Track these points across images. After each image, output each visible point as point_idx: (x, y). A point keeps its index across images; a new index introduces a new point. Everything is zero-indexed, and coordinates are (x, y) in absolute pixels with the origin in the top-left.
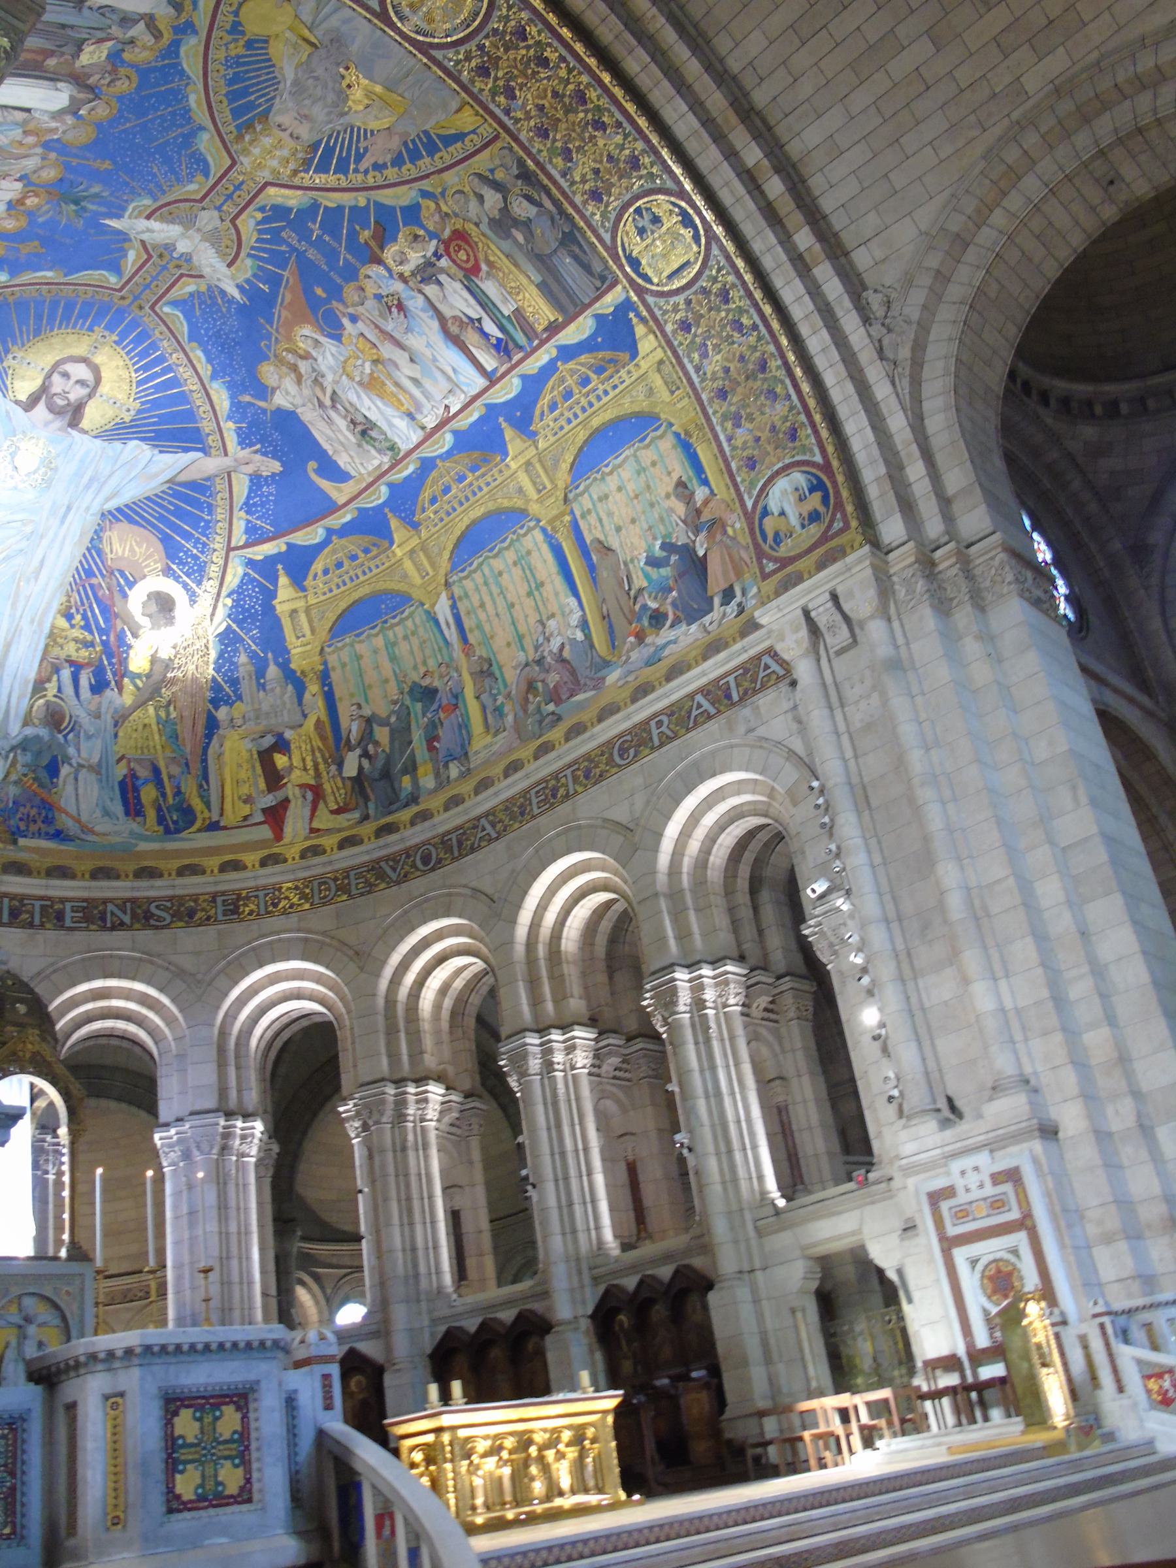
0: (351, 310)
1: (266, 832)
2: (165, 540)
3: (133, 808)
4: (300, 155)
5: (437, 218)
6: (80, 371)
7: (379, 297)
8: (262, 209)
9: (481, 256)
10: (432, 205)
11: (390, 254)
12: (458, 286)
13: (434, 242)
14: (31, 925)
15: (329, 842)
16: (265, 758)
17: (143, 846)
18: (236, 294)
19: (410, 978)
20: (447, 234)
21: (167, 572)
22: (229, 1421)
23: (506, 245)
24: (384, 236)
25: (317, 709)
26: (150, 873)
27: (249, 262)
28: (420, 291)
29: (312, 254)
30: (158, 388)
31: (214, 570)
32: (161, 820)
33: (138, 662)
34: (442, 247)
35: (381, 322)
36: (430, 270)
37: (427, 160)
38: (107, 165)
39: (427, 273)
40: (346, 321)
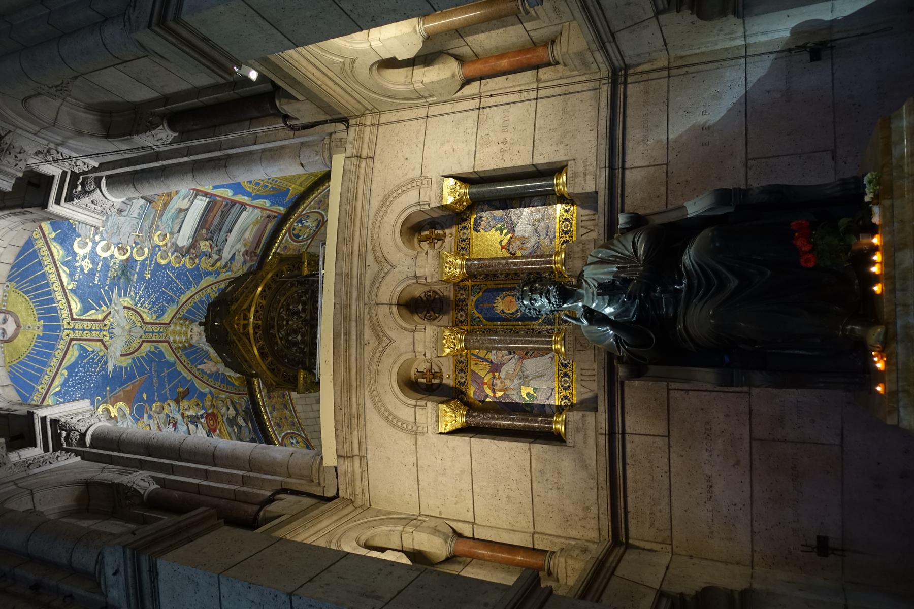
0: (151, 412)
4: (186, 344)
5: (210, 404)
7: (168, 415)
8: (156, 348)
9: (218, 427)
10: (211, 399)
11: (184, 404)
12: (204, 432)
13: (203, 411)
18: (110, 368)
20: (210, 411)
23: (230, 430)
24: (186, 395)
27: (130, 361)
28: (187, 425)
29: (155, 381)
30: (25, 374)
34: (205, 415)
35: (162, 426)
36: (196, 419)
37: (219, 383)
38: (148, 276)
39: (194, 420)
40: (146, 416)
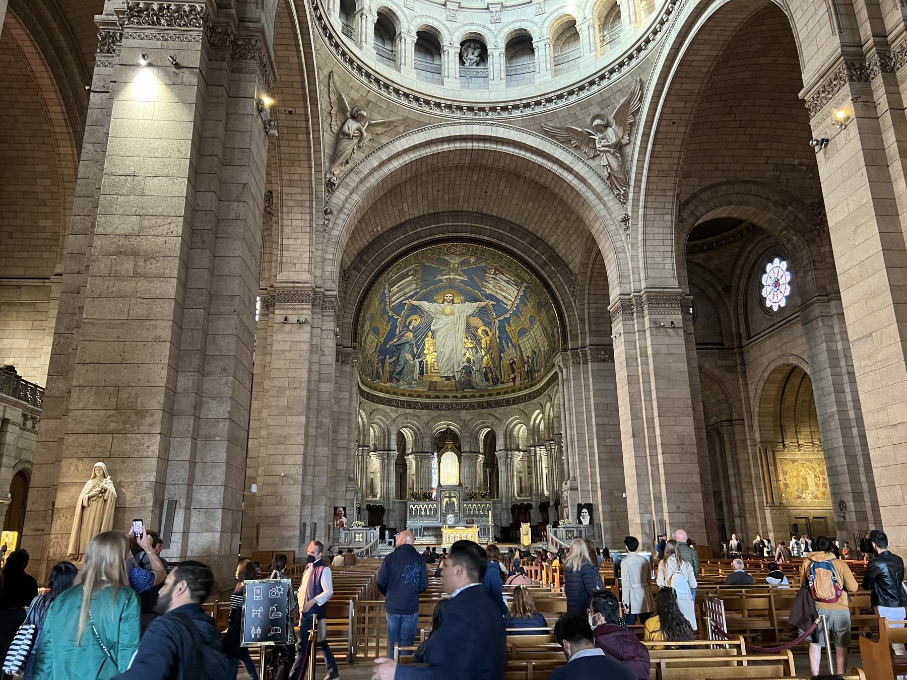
1: (512, 384)
2: (481, 319)
3: (487, 380)
6: (449, 295)
14: (467, 409)
15: (523, 386)
16: (511, 364)
17: (490, 388)
19: (537, 422)
21: (484, 325)
22: (361, 535)
25: (519, 354)
26: (490, 395)
31: (493, 324)
32: (493, 381)
33: (483, 346)
